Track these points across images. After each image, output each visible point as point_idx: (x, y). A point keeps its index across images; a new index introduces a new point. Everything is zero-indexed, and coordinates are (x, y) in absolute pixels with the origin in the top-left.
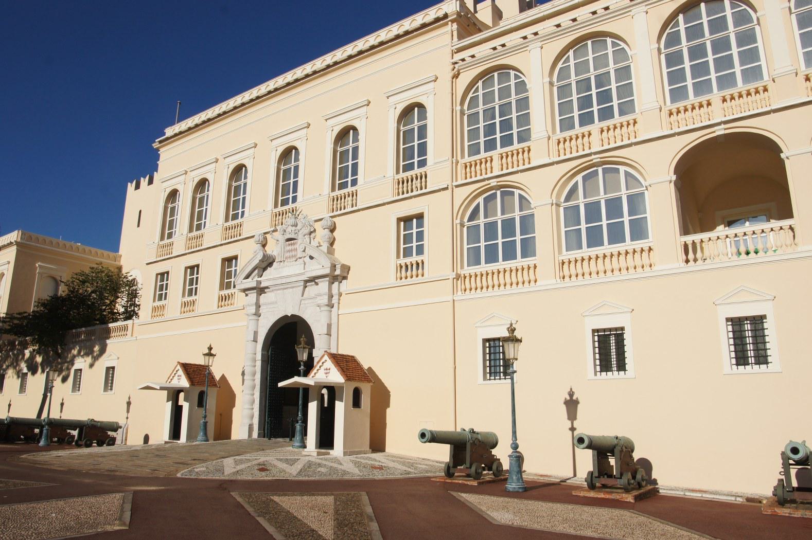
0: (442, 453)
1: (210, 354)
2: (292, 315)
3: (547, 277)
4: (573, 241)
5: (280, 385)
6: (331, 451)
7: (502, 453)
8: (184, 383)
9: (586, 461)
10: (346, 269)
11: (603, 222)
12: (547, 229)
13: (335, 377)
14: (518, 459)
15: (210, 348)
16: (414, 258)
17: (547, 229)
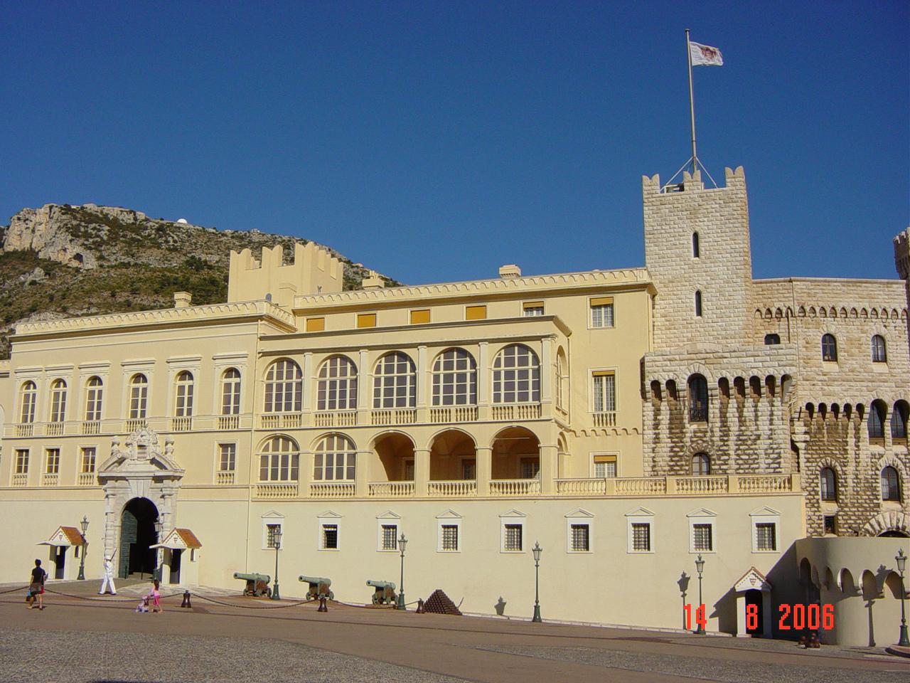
0: (242, 586)
1: (85, 522)
2: (142, 498)
3: (305, 492)
4: (318, 475)
5: (151, 547)
6: (178, 585)
7: (271, 585)
8: (65, 541)
9: (306, 588)
10: (183, 471)
11: (337, 467)
12: (307, 466)
13: (179, 543)
14: (276, 587)
15: (85, 519)
16: (228, 472)
17: (307, 466)
